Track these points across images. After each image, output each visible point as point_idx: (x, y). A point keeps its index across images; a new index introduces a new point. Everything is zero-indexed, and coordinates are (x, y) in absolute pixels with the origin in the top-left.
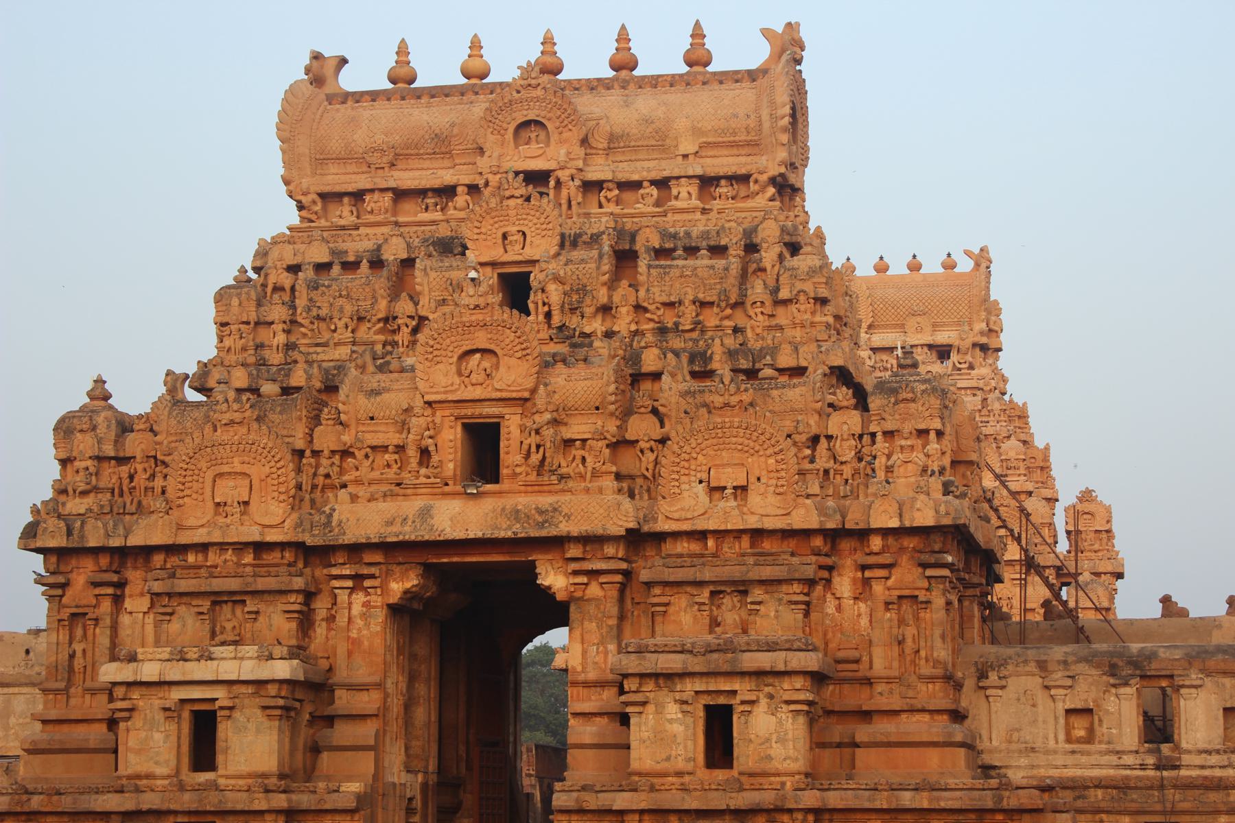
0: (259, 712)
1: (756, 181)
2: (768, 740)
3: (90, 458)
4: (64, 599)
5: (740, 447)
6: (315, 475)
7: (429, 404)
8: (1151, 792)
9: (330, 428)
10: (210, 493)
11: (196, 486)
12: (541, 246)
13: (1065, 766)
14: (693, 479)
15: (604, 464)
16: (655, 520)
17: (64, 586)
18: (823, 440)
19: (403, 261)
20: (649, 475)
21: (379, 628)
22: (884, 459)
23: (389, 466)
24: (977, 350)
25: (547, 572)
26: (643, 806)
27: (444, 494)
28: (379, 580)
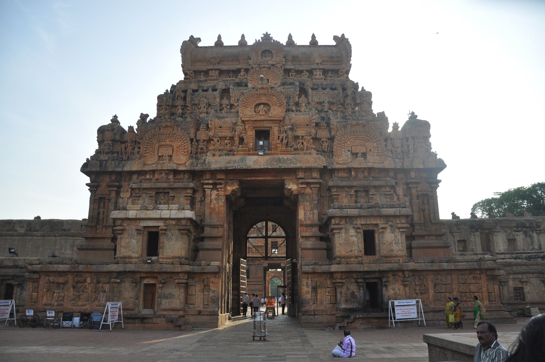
0: (177, 232)
2: (391, 243)
3: (111, 140)
4: (97, 192)
5: (363, 139)
6: (197, 149)
7: (243, 122)
9: (203, 132)
10: (157, 152)
14: (346, 149)
16: (333, 164)
17: (97, 187)
18: (389, 141)
19: (224, 90)
20: (326, 150)
21: (222, 204)
22: (412, 146)
23: (226, 144)
25: (289, 183)
26: (344, 270)
27: (249, 155)
28: (223, 185)
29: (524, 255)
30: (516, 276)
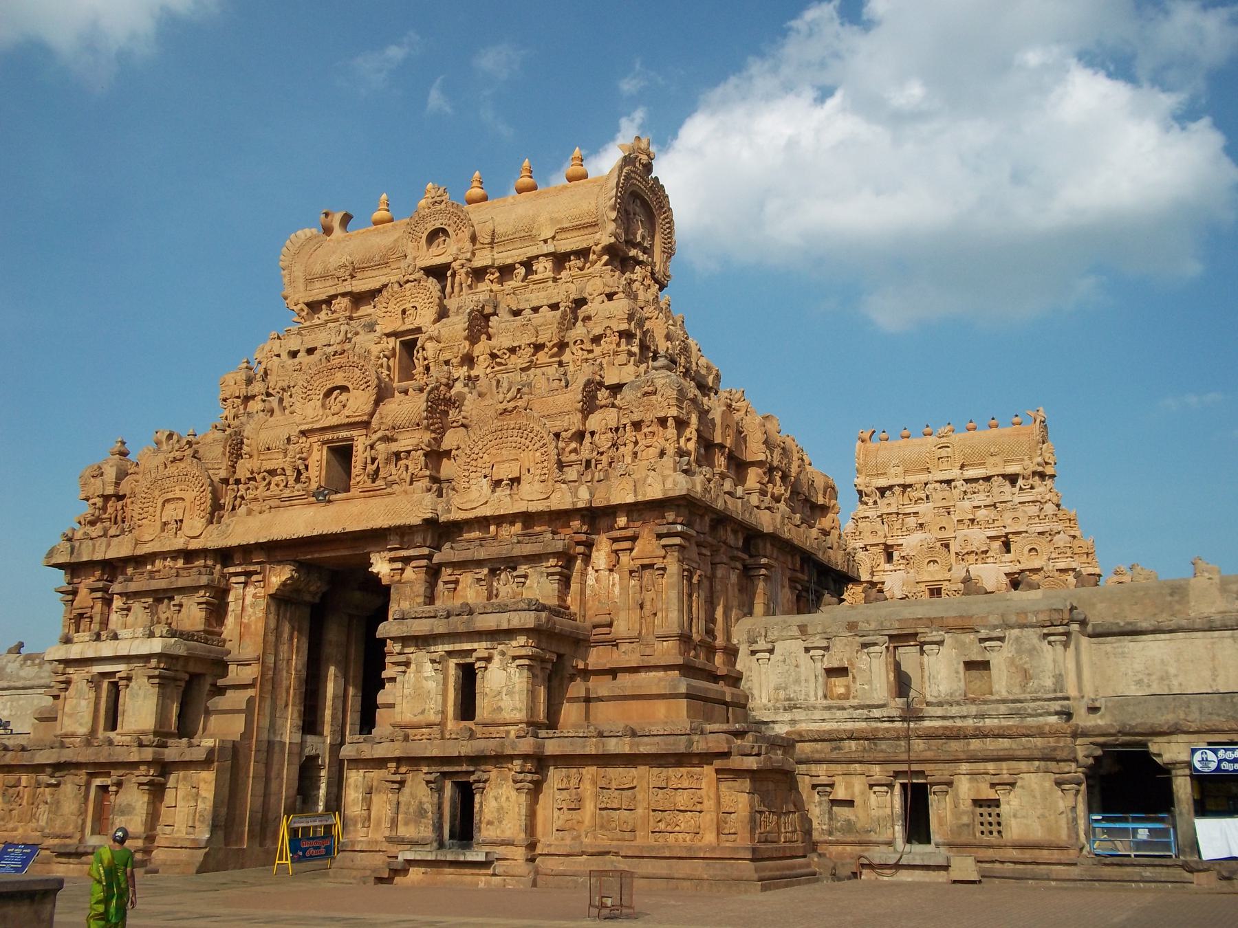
1: (594, 253)
2: (499, 693)
3: (98, 496)
6: (236, 497)
8: (898, 742)
11: (151, 510)
12: (424, 317)
13: (823, 720)
15: (421, 470)
16: (449, 511)
17: (74, 593)
18: (588, 435)
21: (261, 614)
23: (277, 485)
24: (1037, 478)
26: (397, 754)
29: (1003, 708)
30: (981, 767)
